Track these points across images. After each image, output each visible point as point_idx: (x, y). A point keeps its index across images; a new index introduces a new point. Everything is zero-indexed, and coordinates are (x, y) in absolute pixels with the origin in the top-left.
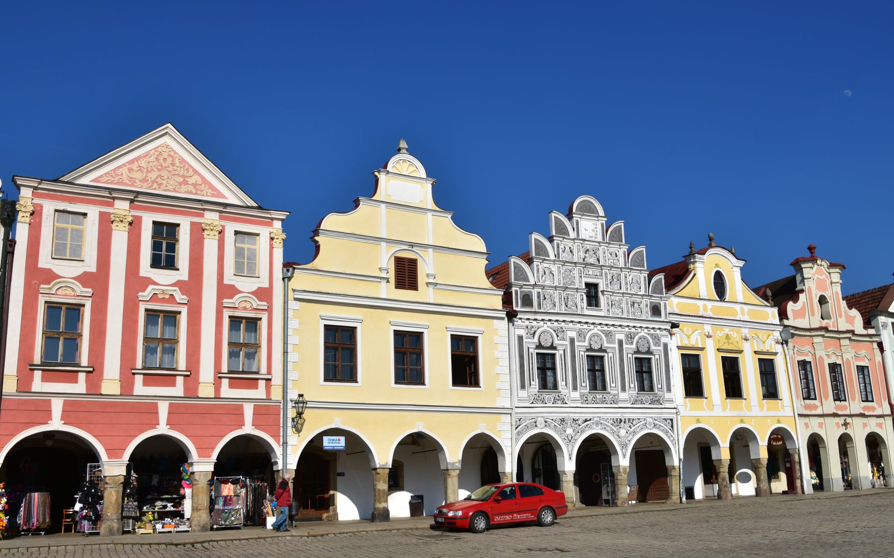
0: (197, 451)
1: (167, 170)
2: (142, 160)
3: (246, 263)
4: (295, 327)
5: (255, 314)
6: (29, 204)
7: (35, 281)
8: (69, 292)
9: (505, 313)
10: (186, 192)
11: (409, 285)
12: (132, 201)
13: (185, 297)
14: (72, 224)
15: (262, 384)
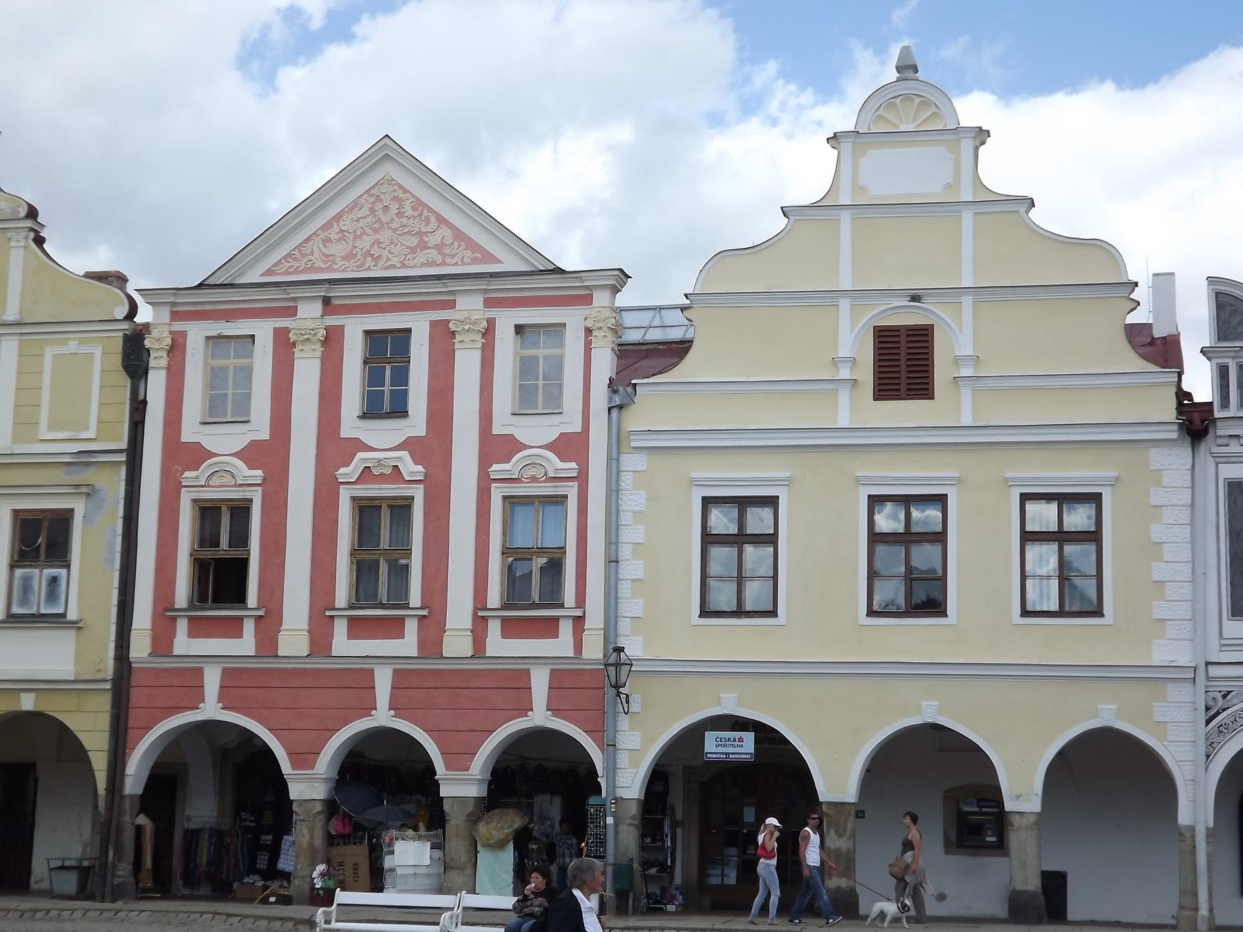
0: (288, 757)
1: (390, 228)
2: (344, 218)
3: (540, 386)
4: (637, 508)
5: (552, 489)
6: (167, 334)
7: (177, 467)
8: (227, 479)
9: (1175, 427)
10: (424, 265)
11: (908, 390)
12: (327, 301)
13: (420, 468)
14: (235, 358)
15: (566, 629)
